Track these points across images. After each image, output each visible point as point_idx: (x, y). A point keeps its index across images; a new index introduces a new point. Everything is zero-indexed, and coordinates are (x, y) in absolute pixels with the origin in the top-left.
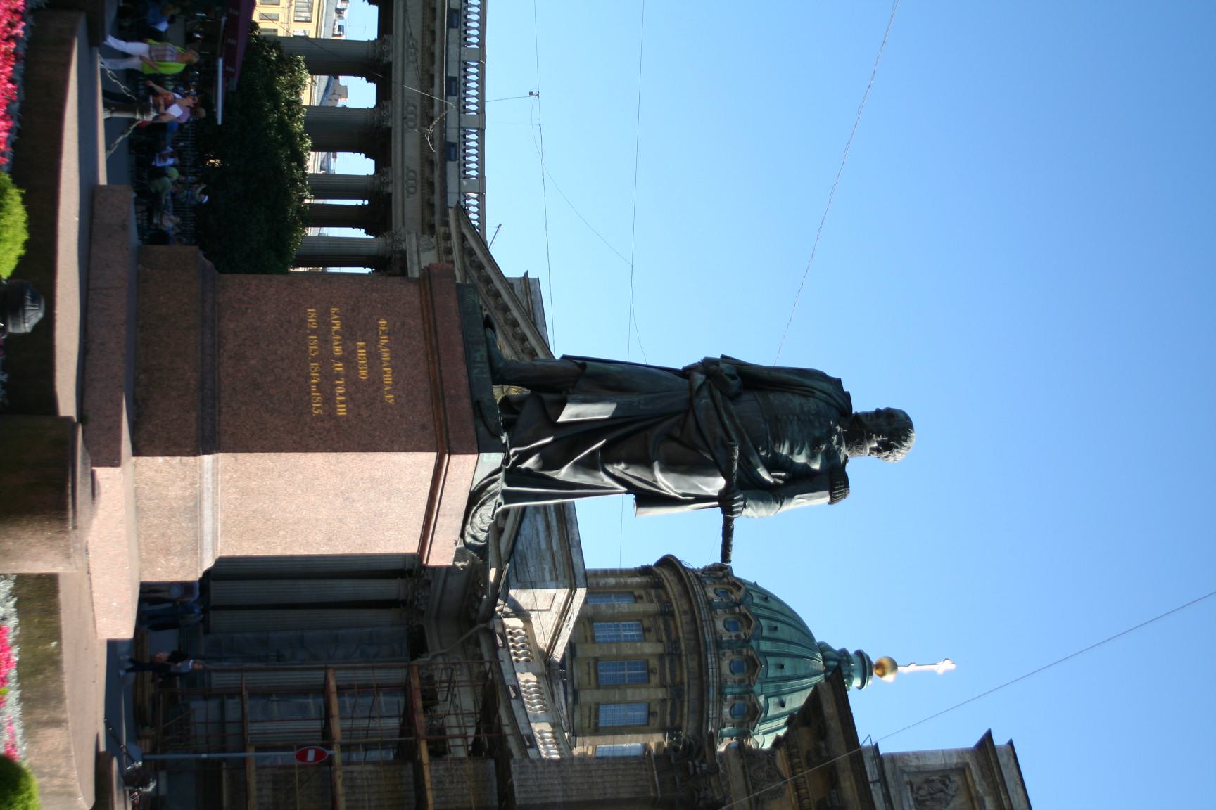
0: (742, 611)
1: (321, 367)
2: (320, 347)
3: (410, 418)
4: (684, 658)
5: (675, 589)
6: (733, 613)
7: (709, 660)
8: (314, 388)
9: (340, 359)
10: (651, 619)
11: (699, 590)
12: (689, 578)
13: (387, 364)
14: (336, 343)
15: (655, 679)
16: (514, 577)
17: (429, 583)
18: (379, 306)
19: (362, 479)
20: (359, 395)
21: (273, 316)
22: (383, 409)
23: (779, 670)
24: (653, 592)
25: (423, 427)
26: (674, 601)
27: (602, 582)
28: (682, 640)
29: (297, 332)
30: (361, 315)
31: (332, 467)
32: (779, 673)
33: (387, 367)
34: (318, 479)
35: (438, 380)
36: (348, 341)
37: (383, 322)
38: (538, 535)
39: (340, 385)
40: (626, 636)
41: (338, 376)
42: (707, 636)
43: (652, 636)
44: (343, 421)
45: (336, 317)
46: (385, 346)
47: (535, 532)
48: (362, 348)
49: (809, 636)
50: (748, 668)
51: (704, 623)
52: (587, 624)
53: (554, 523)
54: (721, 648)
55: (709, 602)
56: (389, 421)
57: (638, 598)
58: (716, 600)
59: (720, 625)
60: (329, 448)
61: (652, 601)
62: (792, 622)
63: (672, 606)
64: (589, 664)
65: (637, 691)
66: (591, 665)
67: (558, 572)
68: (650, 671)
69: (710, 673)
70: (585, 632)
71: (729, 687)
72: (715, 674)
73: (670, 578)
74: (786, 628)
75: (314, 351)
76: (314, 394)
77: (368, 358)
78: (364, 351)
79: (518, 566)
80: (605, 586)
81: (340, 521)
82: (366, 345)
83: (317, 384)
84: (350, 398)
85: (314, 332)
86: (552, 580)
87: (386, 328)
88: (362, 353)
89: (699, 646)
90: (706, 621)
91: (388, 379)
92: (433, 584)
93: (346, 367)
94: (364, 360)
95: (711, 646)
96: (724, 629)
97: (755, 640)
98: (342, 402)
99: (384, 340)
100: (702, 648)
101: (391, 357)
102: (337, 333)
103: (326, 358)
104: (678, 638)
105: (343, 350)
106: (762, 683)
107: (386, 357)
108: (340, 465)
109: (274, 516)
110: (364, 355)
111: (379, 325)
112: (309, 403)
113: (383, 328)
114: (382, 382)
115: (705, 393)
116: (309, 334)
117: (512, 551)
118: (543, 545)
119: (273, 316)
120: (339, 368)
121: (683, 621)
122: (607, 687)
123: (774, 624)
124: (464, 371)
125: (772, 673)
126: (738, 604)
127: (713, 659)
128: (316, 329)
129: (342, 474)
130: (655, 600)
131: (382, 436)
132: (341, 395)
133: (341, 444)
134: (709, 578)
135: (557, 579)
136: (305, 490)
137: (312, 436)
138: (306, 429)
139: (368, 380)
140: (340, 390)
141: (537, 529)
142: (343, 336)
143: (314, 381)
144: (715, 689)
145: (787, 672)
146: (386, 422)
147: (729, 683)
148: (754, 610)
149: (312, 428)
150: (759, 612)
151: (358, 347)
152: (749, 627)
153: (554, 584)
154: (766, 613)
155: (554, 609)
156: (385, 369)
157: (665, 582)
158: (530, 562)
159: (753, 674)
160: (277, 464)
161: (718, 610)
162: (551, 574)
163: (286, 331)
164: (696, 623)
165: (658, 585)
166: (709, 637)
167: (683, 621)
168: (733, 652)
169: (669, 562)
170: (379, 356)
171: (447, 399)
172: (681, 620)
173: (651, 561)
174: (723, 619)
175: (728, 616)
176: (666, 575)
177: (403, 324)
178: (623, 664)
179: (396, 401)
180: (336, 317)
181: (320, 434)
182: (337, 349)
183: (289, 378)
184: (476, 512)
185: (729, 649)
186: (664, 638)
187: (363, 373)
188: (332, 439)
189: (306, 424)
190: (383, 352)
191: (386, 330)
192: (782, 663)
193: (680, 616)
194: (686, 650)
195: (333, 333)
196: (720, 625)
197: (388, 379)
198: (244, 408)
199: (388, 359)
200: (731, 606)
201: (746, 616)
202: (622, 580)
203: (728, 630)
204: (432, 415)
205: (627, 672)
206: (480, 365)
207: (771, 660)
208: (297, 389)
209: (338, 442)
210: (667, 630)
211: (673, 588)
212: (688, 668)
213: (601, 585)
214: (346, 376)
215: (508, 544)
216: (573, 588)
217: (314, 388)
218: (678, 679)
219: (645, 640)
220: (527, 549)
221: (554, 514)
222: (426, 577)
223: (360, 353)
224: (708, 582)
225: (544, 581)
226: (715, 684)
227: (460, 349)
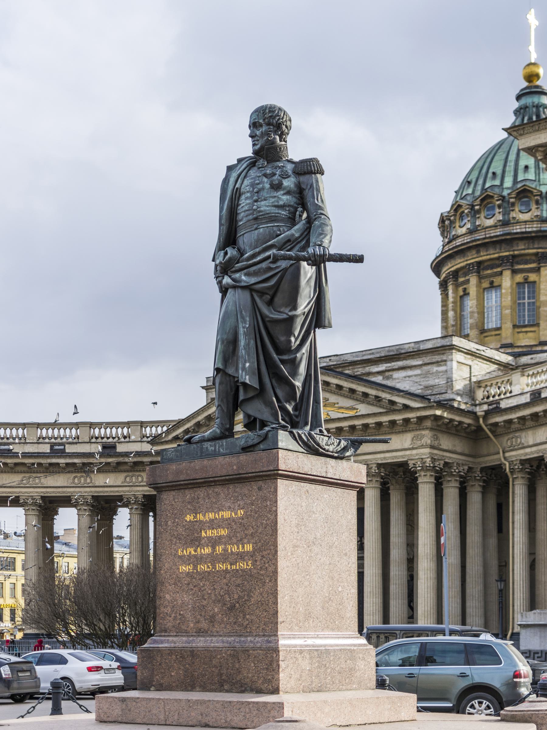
0: (479, 203)
1: (219, 562)
2: (205, 563)
3: (254, 498)
4: (516, 252)
5: (459, 261)
6: (479, 212)
7: (519, 231)
8: (234, 567)
9: (214, 548)
10: (483, 281)
11: (460, 240)
12: (449, 250)
15: (532, 277)
16: (443, 396)
17: (446, 464)
19: (298, 532)
20: (238, 535)
21: (185, 596)
22: (248, 518)
23: (529, 170)
24: (461, 280)
25: (260, 489)
26: (469, 262)
27: (451, 322)
28: (501, 254)
29: (195, 578)
30: (183, 533)
31: (289, 554)
32: (532, 170)
33: (219, 515)
34: (298, 564)
38: (409, 377)
39: (231, 550)
41: (225, 550)
42: (498, 233)
43: (496, 281)
44: (257, 546)
45: (185, 551)
46: (204, 516)
47: (407, 379)
48: (206, 533)
49: (501, 144)
50: (527, 197)
51: (487, 236)
52: (485, 334)
53: (400, 364)
54: (509, 220)
55: (470, 232)
56: (256, 513)
57: (466, 293)
58: (469, 226)
59: (490, 222)
60: (274, 557)
61: (468, 281)
62: (489, 160)
63: (472, 263)
64: (518, 332)
65: (542, 291)
66: (519, 330)
67: (439, 360)
68: (526, 280)
69: (530, 230)
70: (492, 336)
71: (542, 213)
72: (530, 226)
73: (450, 265)
74: (493, 164)
75: (208, 567)
76: (238, 568)
77: (213, 529)
79: (434, 393)
80: (456, 320)
81: (330, 547)
82: (204, 529)
83: (231, 564)
84: (241, 541)
85: (195, 567)
86: (446, 365)
88: (209, 533)
89: (506, 240)
90: (485, 234)
92: (447, 460)
93: (220, 543)
95: (507, 229)
96: (493, 219)
97: (502, 192)
98: (243, 547)
99: (200, 517)
100: (508, 237)
101: (212, 512)
102: (195, 551)
103: (213, 559)
104: (498, 258)
105: (207, 546)
106: (540, 185)
107: (211, 516)
108: (287, 549)
109: (327, 595)
111: (190, 521)
112: (243, 570)
113: (192, 517)
114: (229, 518)
116: (197, 571)
117: (422, 397)
118: (418, 372)
119: (185, 596)
120: (219, 549)
121: (485, 253)
122: (539, 318)
123: (490, 175)
124: (221, 459)
125: (531, 175)
126: (472, 206)
127: (518, 227)
128: (193, 565)
129: (295, 546)
130: (467, 278)
132: (238, 548)
133: (272, 547)
134: (449, 232)
135: (445, 361)
136: (307, 573)
137: (266, 568)
138: (262, 572)
139: (228, 528)
140: (235, 549)
141: (405, 377)
142: (198, 546)
143: (229, 567)
144: (543, 225)
147: (539, 214)
148: (478, 193)
149: (261, 568)
150: (479, 188)
152: (492, 197)
153: (448, 363)
154: (481, 182)
155: (469, 362)
157: (452, 269)
158: (431, 382)
159: (531, 192)
160: (287, 593)
161: (477, 223)
162: (441, 365)
163: (195, 587)
164: (487, 243)
165: (455, 274)
166: (499, 232)
167: (485, 253)
168: (513, 210)
169: (437, 268)
170: (212, 521)
171: (241, 472)
172: (484, 256)
173: (435, 281)
174: (484, 220)
175: (482, 215)
176: (447, 269)
177: (189, 503)
178: (519, 304)
179: (242, 509)
180: (185, 551)
181: (264, 563)
182: (207, 551)
183: (227, 585)
184: (324, 449)
185: (509, 214)
186: (499, 269)
187: (223, 532)
188: (269, 554)
189: (258, 573)
192: (523, 167)
193: (481, 256)
194: (509, 251)
196: (490, 222)
197: (226, 514)
198: (248, 616)
200: (474, 213)
201: (482, 200)
202: (450, 306)
203: (494, 215)
204: (252, 483)
205: (526, 301)
207: (520, 177)
208: (234, 579)
209: (271, 550)
210: (492, 267)
211: (459, 263)
212: (524, 249)
213: (454, 323)
214: (225, 545)
215: (415, 401)
216: (451, 347)
217: (234, 567)
218: (533, 258)
219: (500, 286)
220: (420, 385)
221: (393, 364)
222: (441, 466)
224: (453, 233)
225: (446, 371)
226: (539, 225)
227: (206, 462)
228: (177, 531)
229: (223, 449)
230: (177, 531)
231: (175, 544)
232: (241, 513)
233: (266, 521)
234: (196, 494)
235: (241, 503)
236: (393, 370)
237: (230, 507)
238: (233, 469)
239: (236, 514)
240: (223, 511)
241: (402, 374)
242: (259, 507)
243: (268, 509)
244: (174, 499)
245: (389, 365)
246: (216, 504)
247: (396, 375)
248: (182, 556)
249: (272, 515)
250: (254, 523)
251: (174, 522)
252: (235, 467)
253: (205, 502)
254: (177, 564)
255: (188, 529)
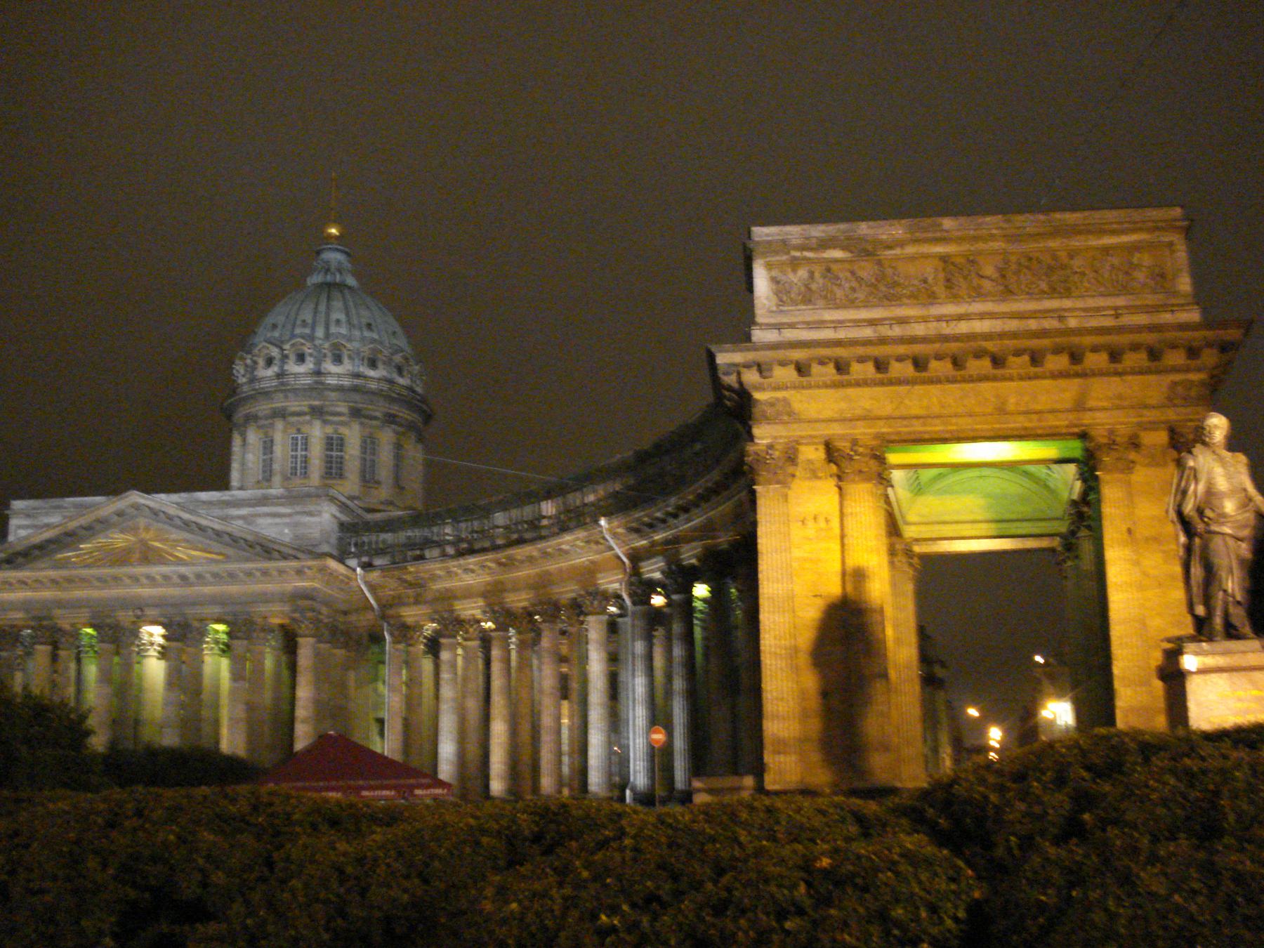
4: (327, 403)
40: (302, 450)
118: (287, 520)
123: (299, 322)
141: (271, 524)
145: (342, 317)
207: (333, 329)
236: (259, 515)
241: (269, 520)
245: (251, 509)
247: (261, 521)
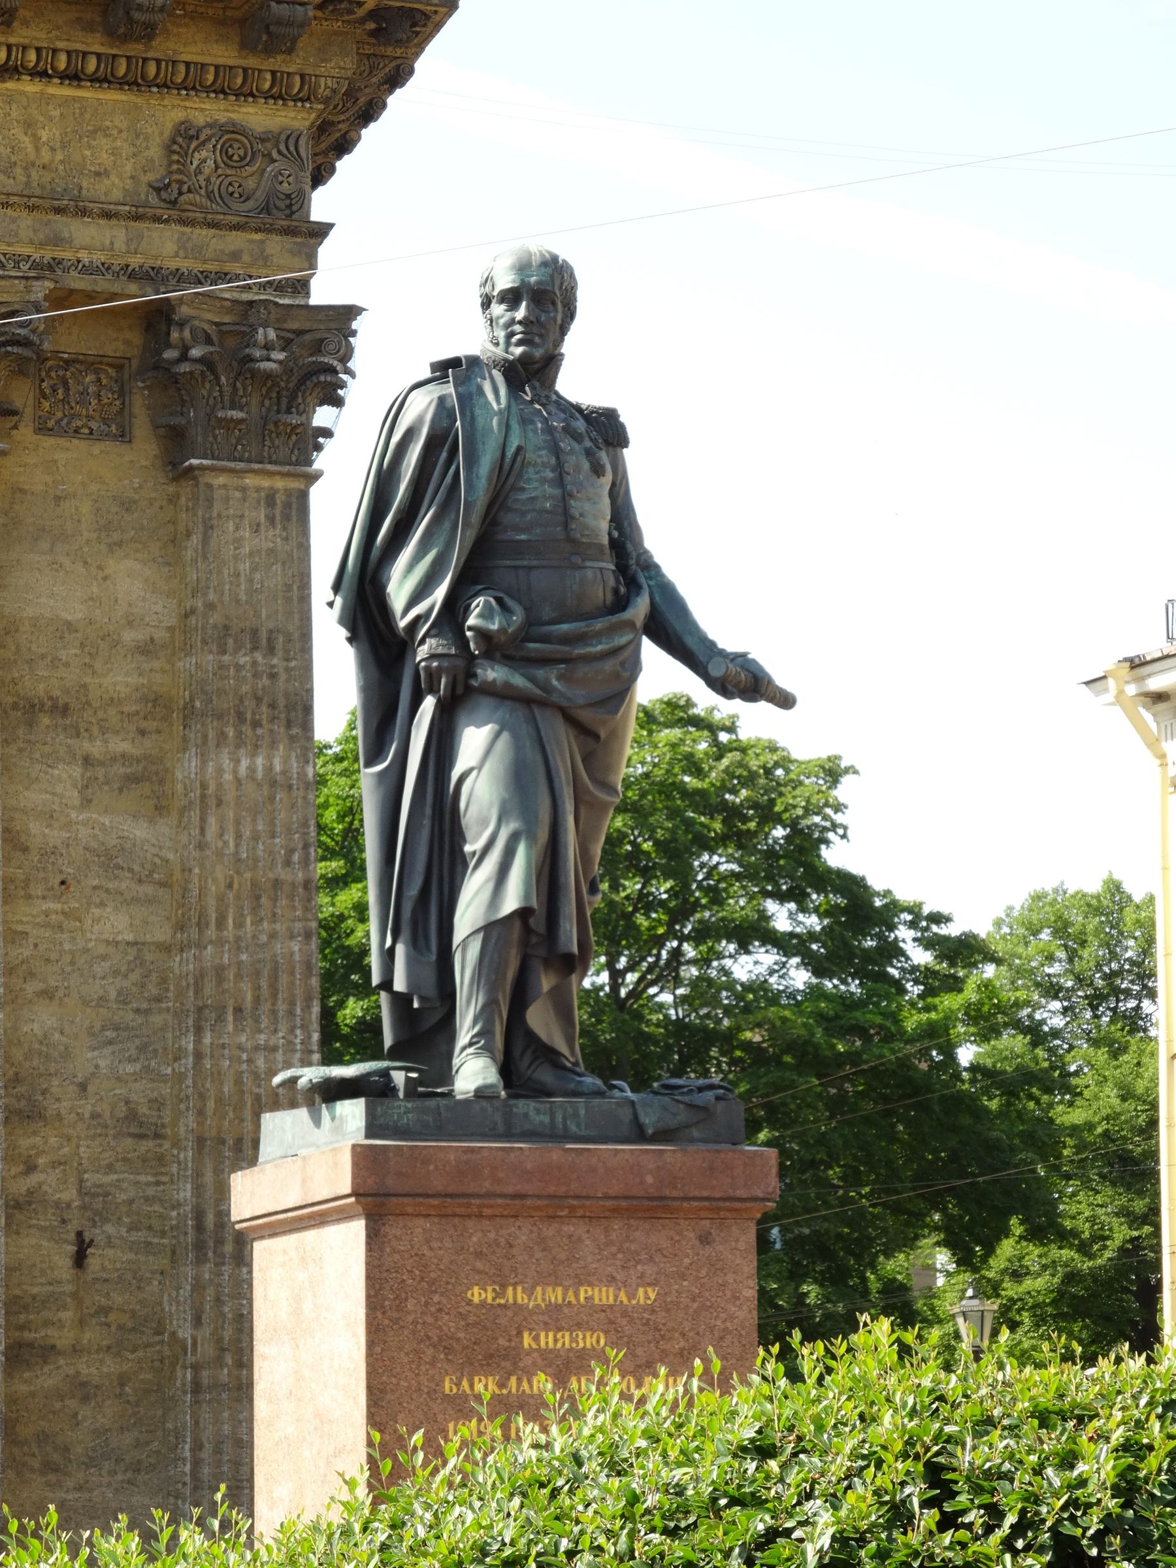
3: (687, 1261)
13: (571, 1293)
14: (525, 1385)
18: (436, 1298)
22: (668, 1311)
30: (461, 1335)
33: (577, 1295)
35: (624, 1203)
36: (521, 1365)
37: (476, 1295)
45: (465, 1384)
46: (530, 1293)
48: (536, 1339)
56: (694, 1300)
77: (559, 1329)
78: (543, 1335)
82: (531, 1330)
87: (490, 1289)
88: (547, 1340)
91: (603, 1295)
94: (563, 1337)
99: (516, 1295)
107: (555, 1295)
110: (551, 1335)
111: (483, 1304)
114: (611, 1307)
115: (540, 673)
131: (723, 1315)
139: (606, 1332)
142: (510, 1374)
146: (695, 1305)
151: (534, 1346)
156: (582, 1299)
170: (554, 1309)
171: (667, 1193)
177: (479, 1255)
179: (649, 1285)
190: (544, 1300)
191: (494, 1290)
195: (505, 1392)
197: (603, 1295)
199: (559, 1290)
206: (559, 1118)
223: (547, 1343)
228: (440, 1328)
229: (578, 1125)
230: (440, 1328)
231: (433, 1363)
232: (646, 1295)
233: (724, 1321)
234: (504, 1232)
235: (650, 1270)
237: (614, 1278)
238: (642, 1183)
239: (631, 1296)
240: (591, 1284)
242: (702, 1285)
243: (728, 1293)
244: (428, 1241)
246: (569, 1266)
248: (457, 1396)
249: (740, 1307)
250: (687, 1326)
251: (427, 1304)
252: (649, 1179)
253: (532, 1256)
254: (440, 1417)
255: (475, 1324)
